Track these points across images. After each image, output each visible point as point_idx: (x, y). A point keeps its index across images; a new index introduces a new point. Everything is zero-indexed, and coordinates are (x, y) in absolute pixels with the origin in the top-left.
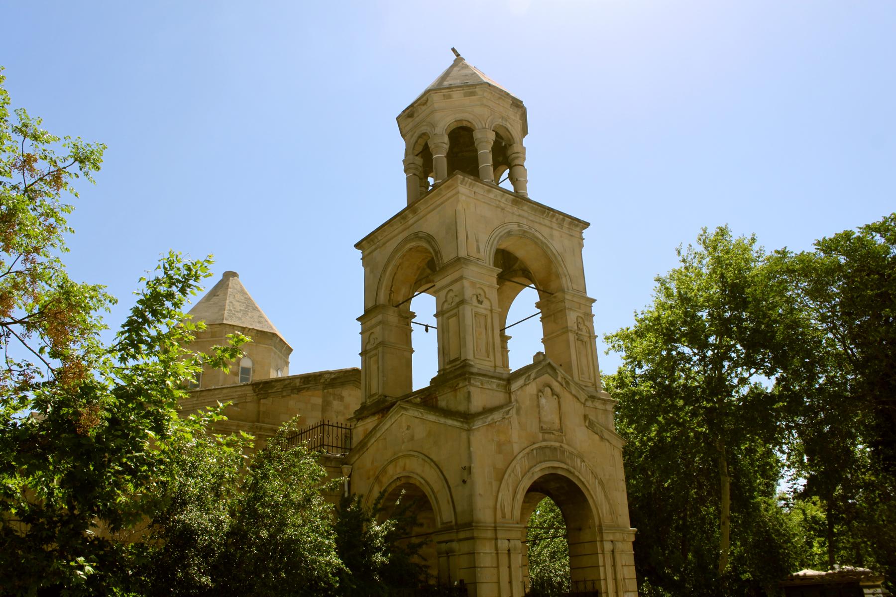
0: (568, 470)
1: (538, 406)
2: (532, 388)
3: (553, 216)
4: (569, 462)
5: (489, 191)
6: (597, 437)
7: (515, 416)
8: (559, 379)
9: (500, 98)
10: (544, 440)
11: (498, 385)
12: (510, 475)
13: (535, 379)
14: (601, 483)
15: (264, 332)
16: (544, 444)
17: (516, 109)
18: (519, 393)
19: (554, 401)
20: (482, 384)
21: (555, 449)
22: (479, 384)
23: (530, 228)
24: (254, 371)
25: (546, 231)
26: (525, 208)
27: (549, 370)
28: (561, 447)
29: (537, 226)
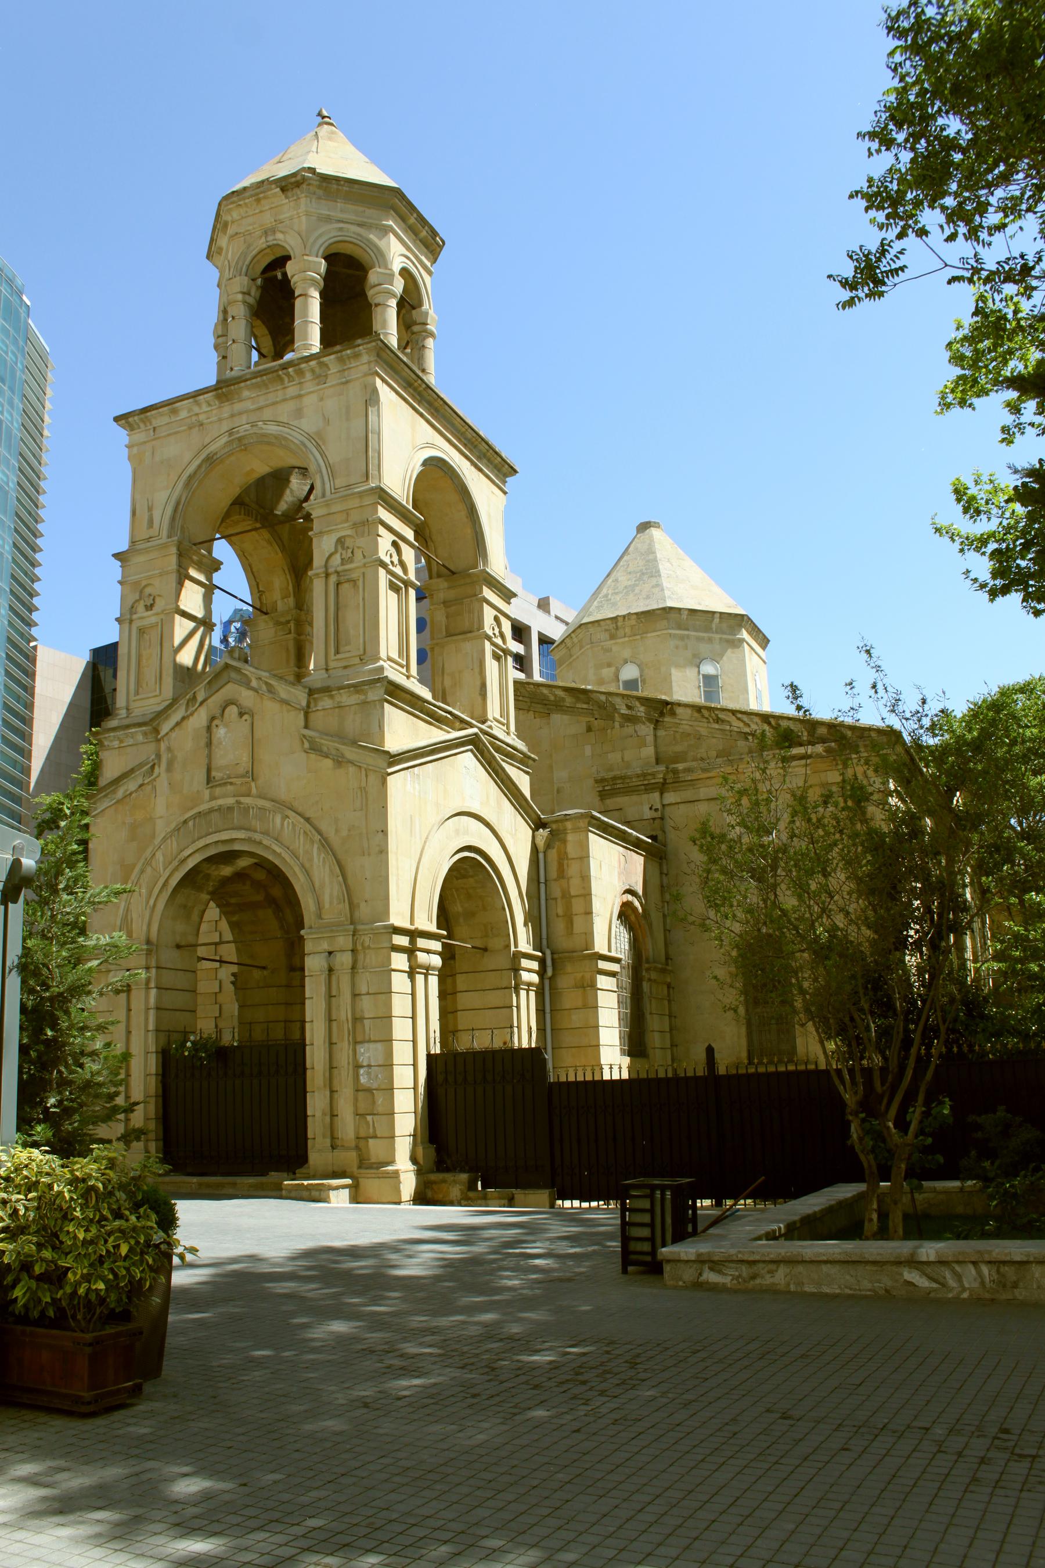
0: (249, 840)
1: (209, 744)
2: (200, 718)
3: (301, 373)
4: (257, 824)
5: (175, 412)
6: (328, 763)
7: (164, 775)
8: (254, 683)
9: (258, 201)
10: (213, 798)
11: (145, 734)
12: (142, 871)
13: (201, 703)
14: (326, 844)
15: (649, 611)
16: (215, 804)
17: (297, 191)
18: (173, 735)
19: (242, 727)
20: (121, 742)
21: (230, 809)
22: (116, 744)
23: (253, 425)
24: (644, 681)
25: (284, 412)
26: (246, 393)
27: (233, 675)
28: (238, 802)
29: (267, 414)
